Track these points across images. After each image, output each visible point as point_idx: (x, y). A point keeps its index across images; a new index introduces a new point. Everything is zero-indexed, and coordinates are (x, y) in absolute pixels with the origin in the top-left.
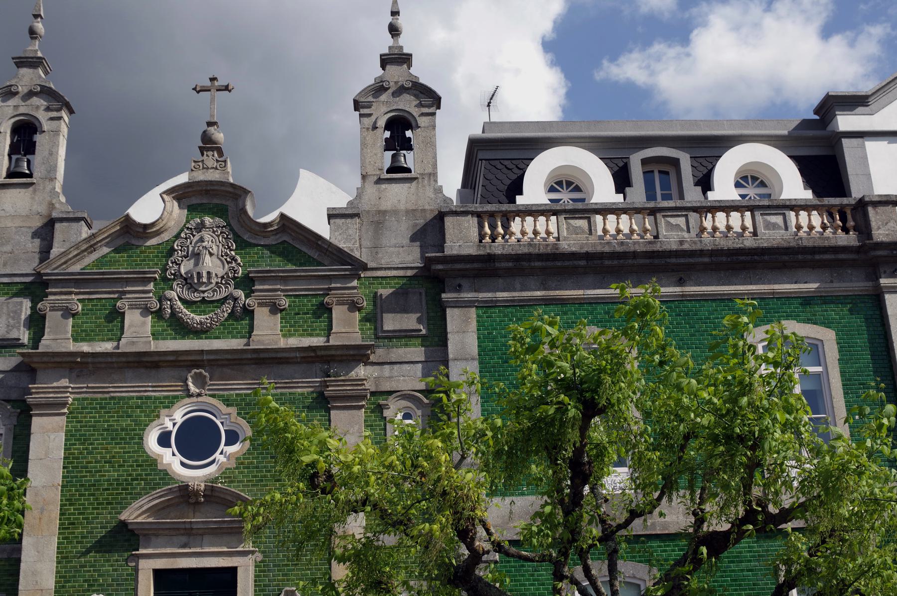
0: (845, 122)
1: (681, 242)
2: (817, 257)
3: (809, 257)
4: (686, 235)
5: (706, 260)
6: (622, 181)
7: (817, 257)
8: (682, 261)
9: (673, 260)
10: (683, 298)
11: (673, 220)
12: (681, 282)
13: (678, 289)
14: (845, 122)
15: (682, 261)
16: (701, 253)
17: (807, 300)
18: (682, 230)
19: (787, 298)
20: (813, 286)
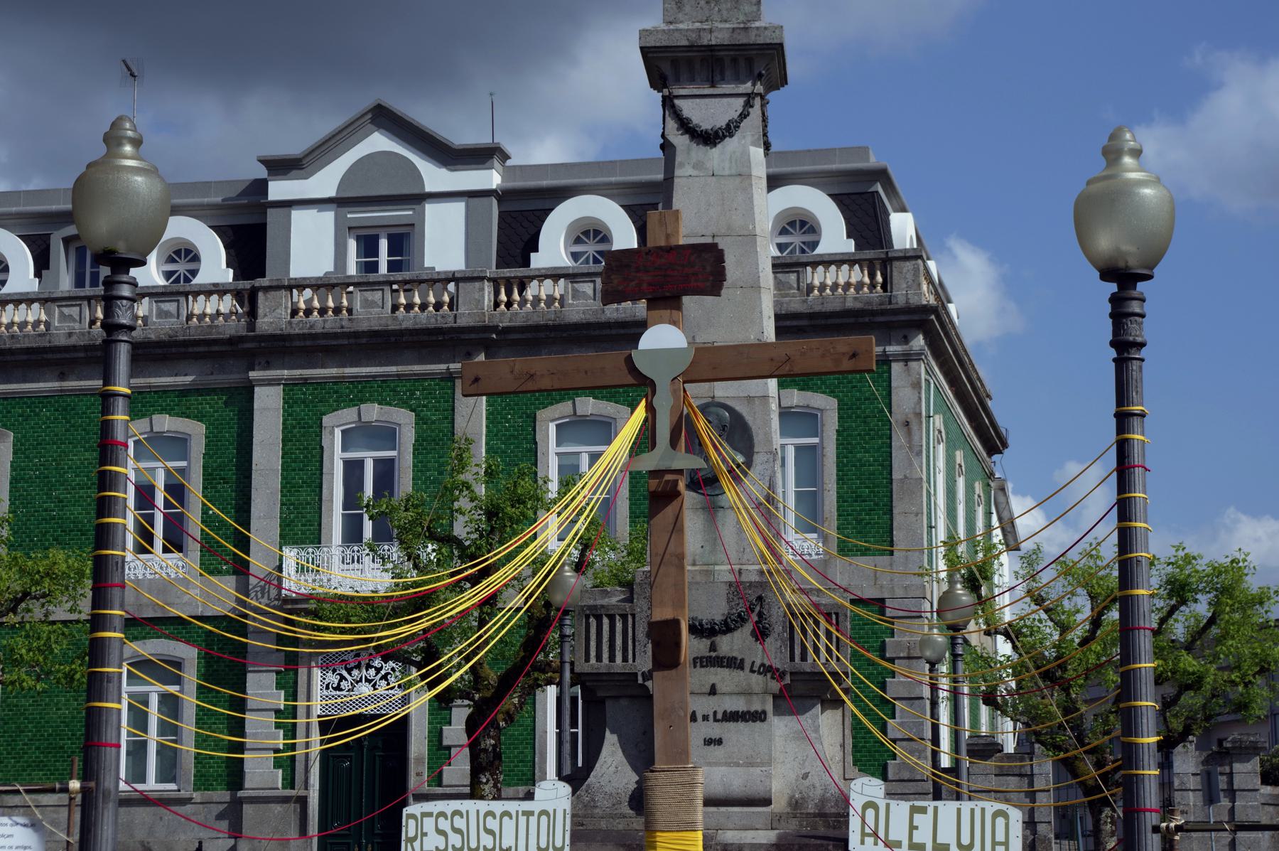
0: (279, 190)
1: (70, 335)
2: (190, 350)
3: (183, 350)
4: (77, 325)
5: (82, 355)
6: (42, 263)
7: (190, 350)
8: (58, 356)
9: (50, 356)
10: (63, 393)
11: (66, 311)
12: (62, 377)
13: (55, 385)
14: (279, 190)
15: (58, 356)
16: (74, 348)
17: (184, 392)
18: (74, 320)
19: (163, 392)
20: (190, 378)
